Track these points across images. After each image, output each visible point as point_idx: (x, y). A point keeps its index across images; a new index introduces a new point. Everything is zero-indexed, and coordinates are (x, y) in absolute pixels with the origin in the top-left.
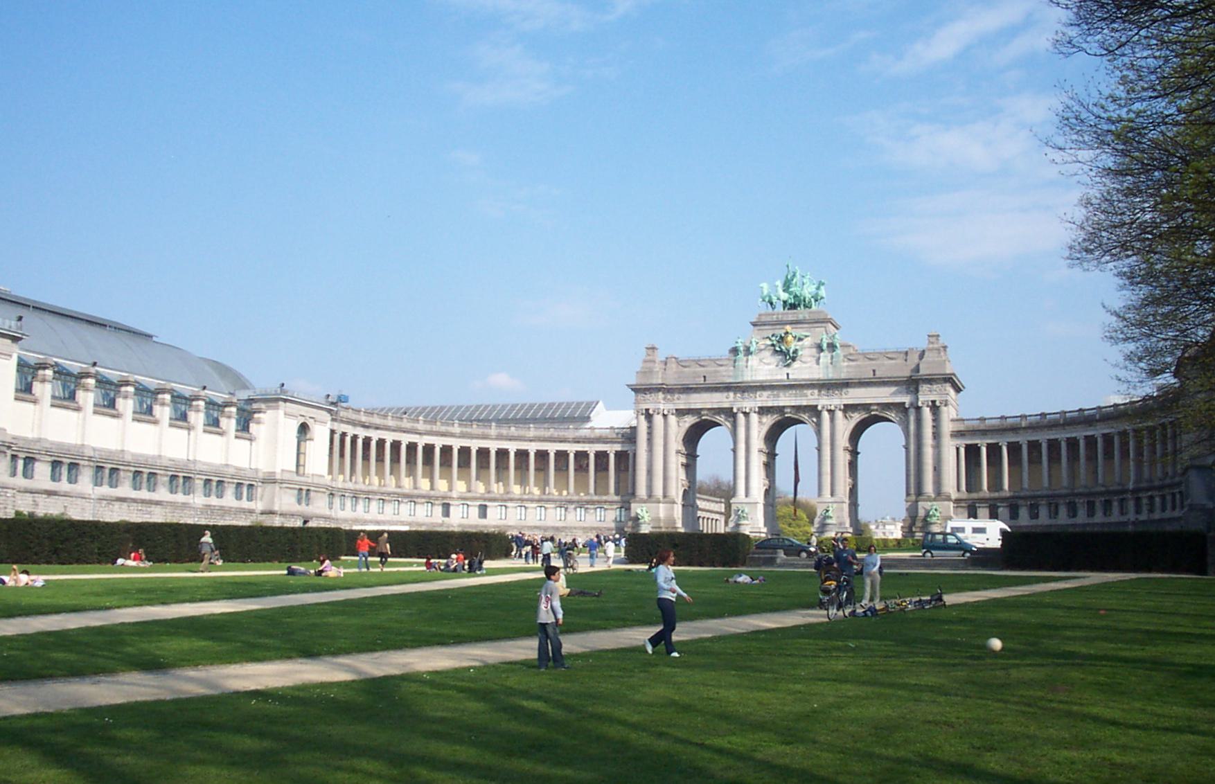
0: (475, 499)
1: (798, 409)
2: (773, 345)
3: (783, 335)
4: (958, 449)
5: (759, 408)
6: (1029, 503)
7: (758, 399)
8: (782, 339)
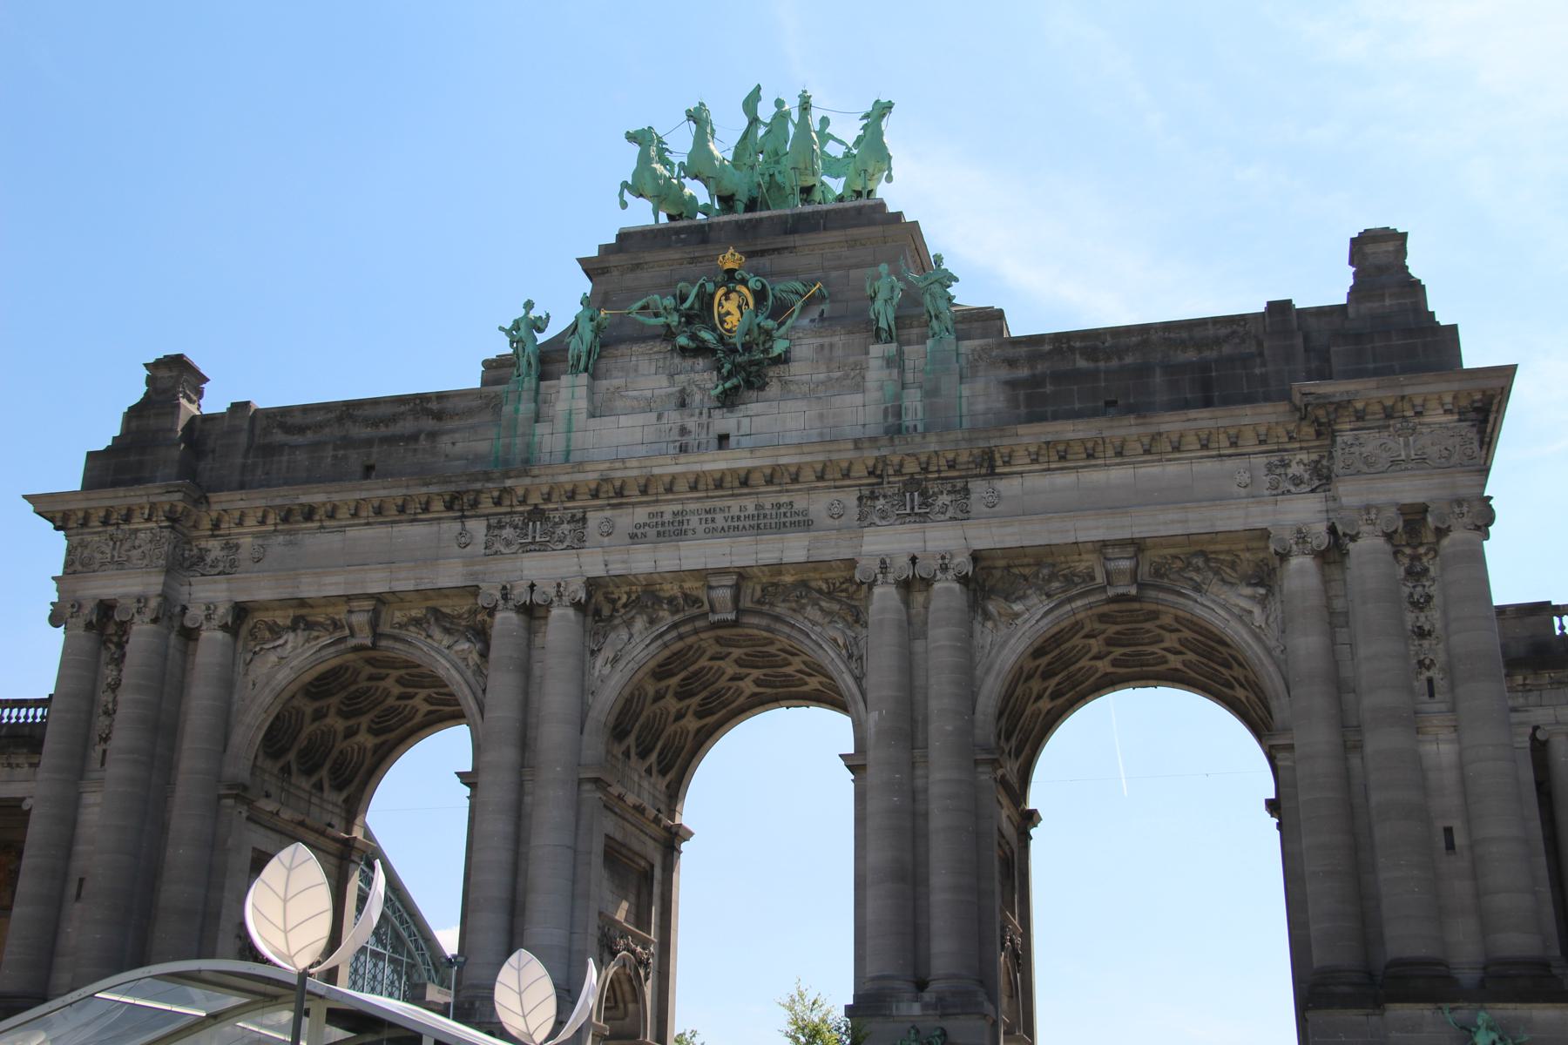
2: (668, 334)
3: (710, 287)
8: (703, 312)
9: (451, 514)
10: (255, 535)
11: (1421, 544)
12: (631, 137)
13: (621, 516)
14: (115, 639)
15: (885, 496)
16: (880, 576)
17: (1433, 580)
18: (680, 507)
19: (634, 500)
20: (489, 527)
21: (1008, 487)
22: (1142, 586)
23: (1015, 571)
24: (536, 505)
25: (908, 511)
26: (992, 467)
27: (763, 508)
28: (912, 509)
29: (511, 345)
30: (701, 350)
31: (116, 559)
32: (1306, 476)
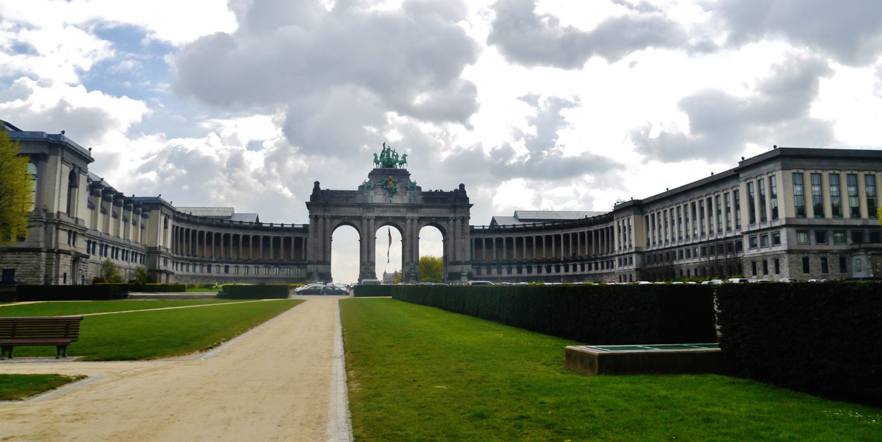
0: (222, 262)
2: (382, 185)
4: (471, 240)
5: (376, 217)
6: (507, 266)
7: (376, 212)
8: (387, 183)
12: (374, 155)
21: (422, 210)
30: (387, 189)
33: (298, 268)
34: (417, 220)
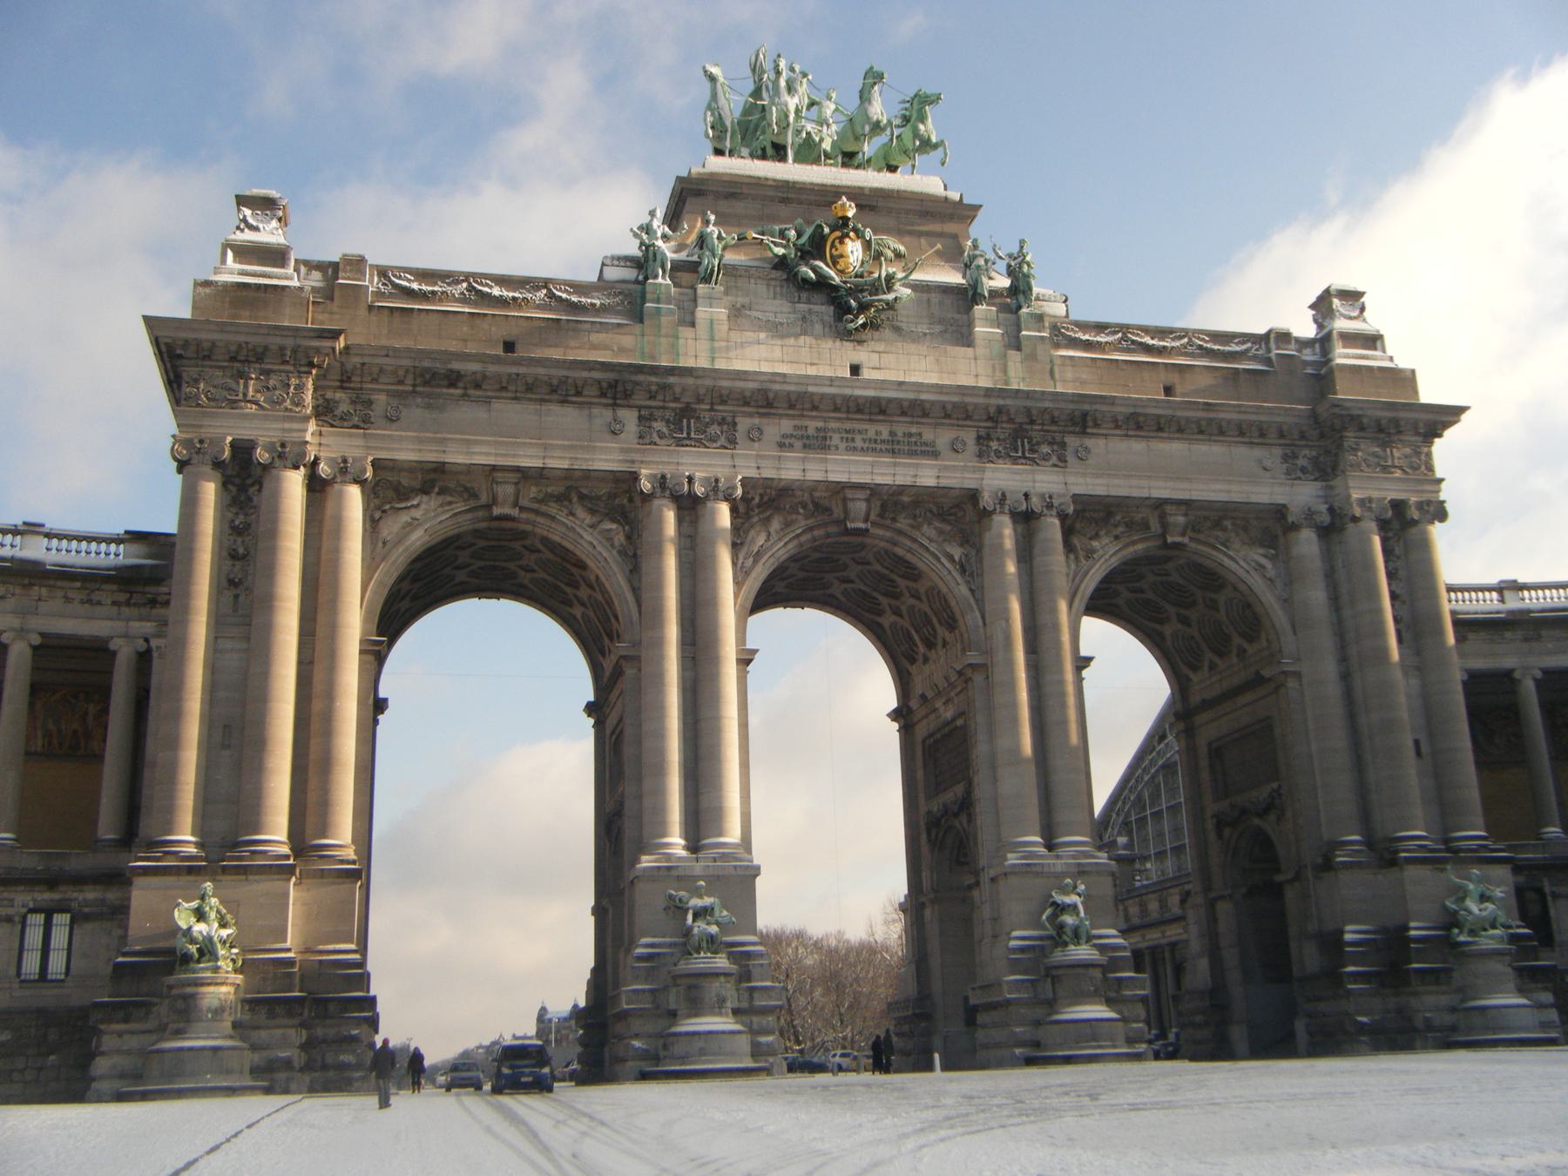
1: (889, 502)
2: (781, 263)
3: (827, 230)
9: (604, 401)
10: (391, 394)
11: (1391, 530)
13: (768, 424)
14: (237, 481)
15: (998, 439)
16: (998, 507)
17: (1398, 558)
18: (820, 424)
19: (781, 411)
20: (640, 418)
21: (1097, 445)
22: (1191, 539)
23: (1087, 515)
24: (688, 403)
25: (1020, 454)
26: (1085, 427)
27: (896, 435)
28: (1023, 452)
29: (640, 247)
31: (249, 398)
32: (1310, 468)
33: (49, 913)
34: (1063, 517)
